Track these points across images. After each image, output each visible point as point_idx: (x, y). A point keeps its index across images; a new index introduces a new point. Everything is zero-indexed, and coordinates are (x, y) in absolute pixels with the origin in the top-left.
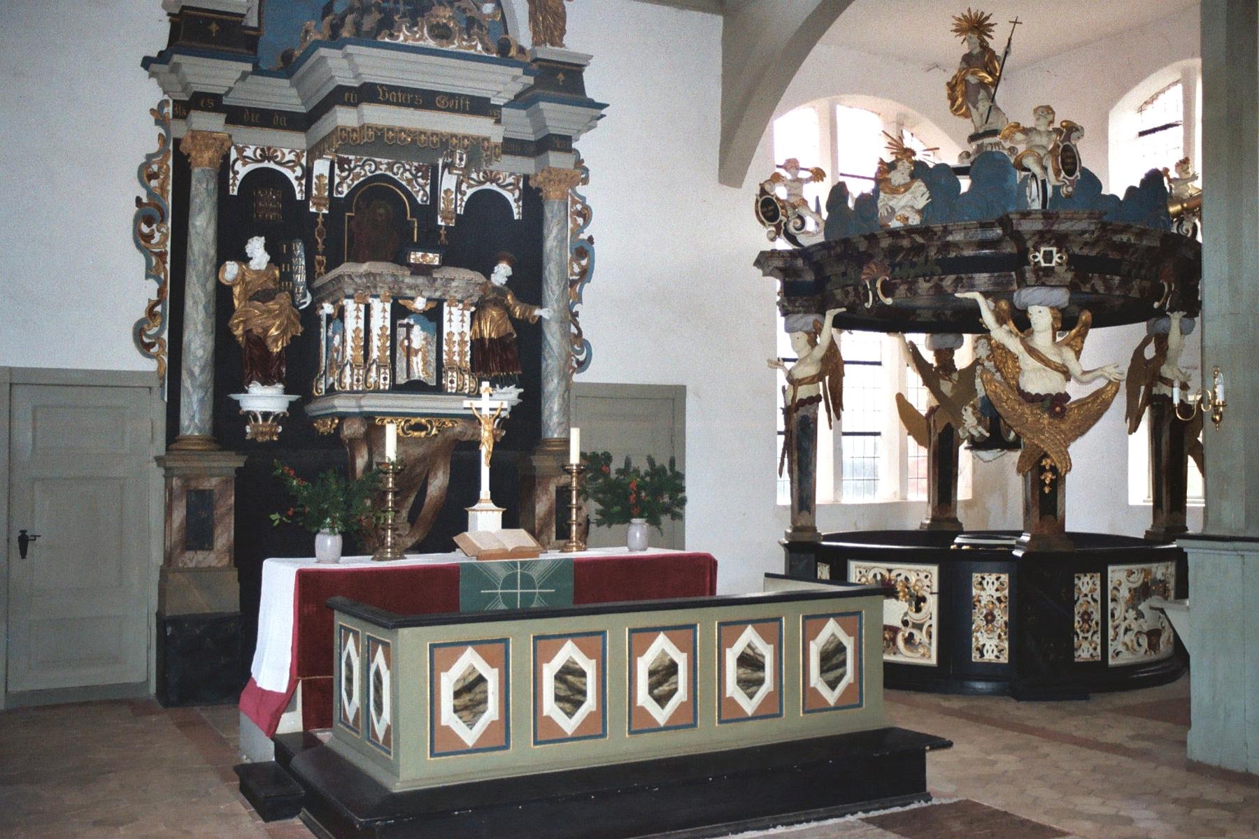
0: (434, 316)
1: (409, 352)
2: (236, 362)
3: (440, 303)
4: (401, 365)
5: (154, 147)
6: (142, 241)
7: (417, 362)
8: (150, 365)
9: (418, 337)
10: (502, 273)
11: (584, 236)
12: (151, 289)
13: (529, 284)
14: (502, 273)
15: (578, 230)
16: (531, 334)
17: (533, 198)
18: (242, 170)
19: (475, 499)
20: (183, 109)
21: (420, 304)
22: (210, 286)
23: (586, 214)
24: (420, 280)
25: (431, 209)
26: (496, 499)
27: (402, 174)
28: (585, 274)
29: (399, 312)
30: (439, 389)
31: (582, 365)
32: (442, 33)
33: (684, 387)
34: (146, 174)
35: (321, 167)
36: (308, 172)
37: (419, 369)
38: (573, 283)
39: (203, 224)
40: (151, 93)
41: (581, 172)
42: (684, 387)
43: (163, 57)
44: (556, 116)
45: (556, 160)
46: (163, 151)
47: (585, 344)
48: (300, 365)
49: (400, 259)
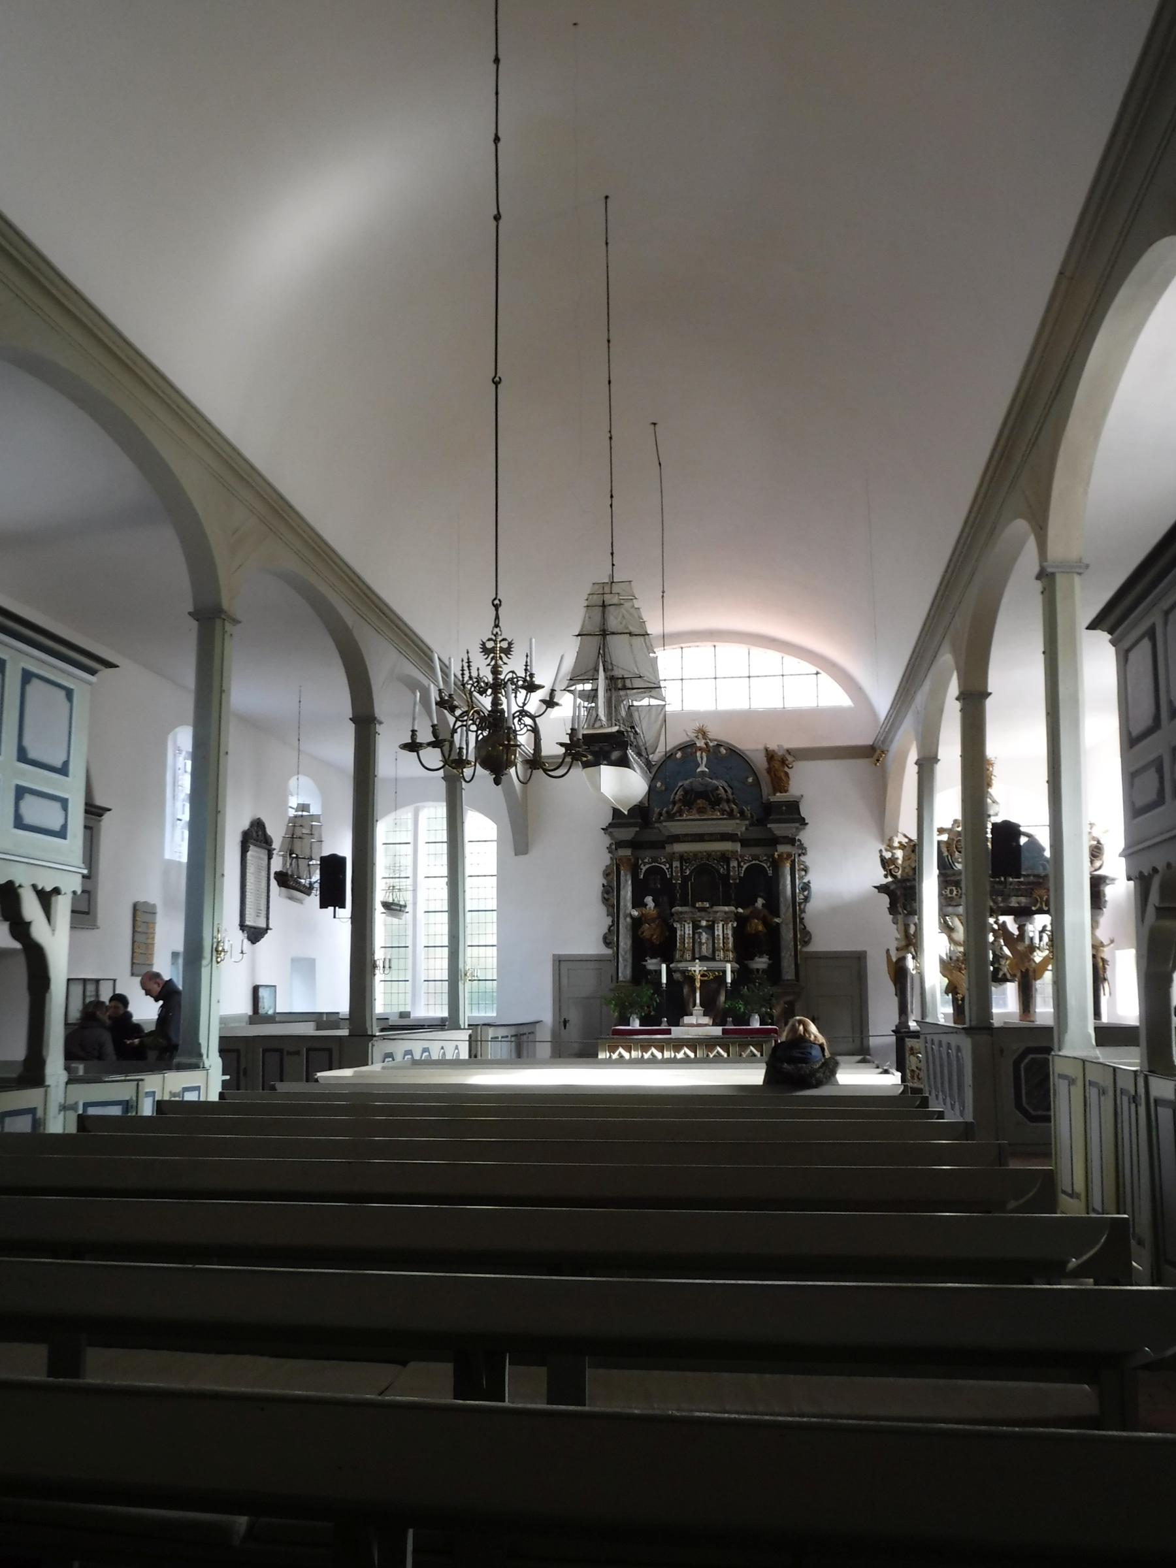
0: (711, 929)
1: (701, 944)
2: (641, 950)
3: (714, 922)
4: (697, 950)
5: (608, 862)
6: (605, 901)
7: (704, 947)
8: (609, 952)
9: (704, 937)
10: (760, 902)
11: (805, 881)
12: (609, 921)
13: (773, 906)
14: (760, 902)
15: (801, 878)
16: (774, 932)
17: (776, 865)
18: (644, 868)
19: (695, 1005)
20: (619, 844)
21: (704, 923)
22: (628, 919)
23: (806, 870)
24: (703, 914)
25: (727, 877)
26: (701, 1005)
27: (714, 864)
28: (806, 899)
29: (696, 926)
30: (713, 959)
31: (806, 944)
32: (701, 811)
33: (865, 952)
34: (607, 874)
35: (676, 864)
36: (671, 866)
37: (705, 951)
38: (800, 904)
39: (627, 893)
40: (606, 841)
41: (803, 851)
42: (865, 952)
43: (611, 825)
44: (779, 829)
45: (782, 849)
46: (612, 864)
47: (808, 933)
48: (667, 951)
49: (694, 906)
